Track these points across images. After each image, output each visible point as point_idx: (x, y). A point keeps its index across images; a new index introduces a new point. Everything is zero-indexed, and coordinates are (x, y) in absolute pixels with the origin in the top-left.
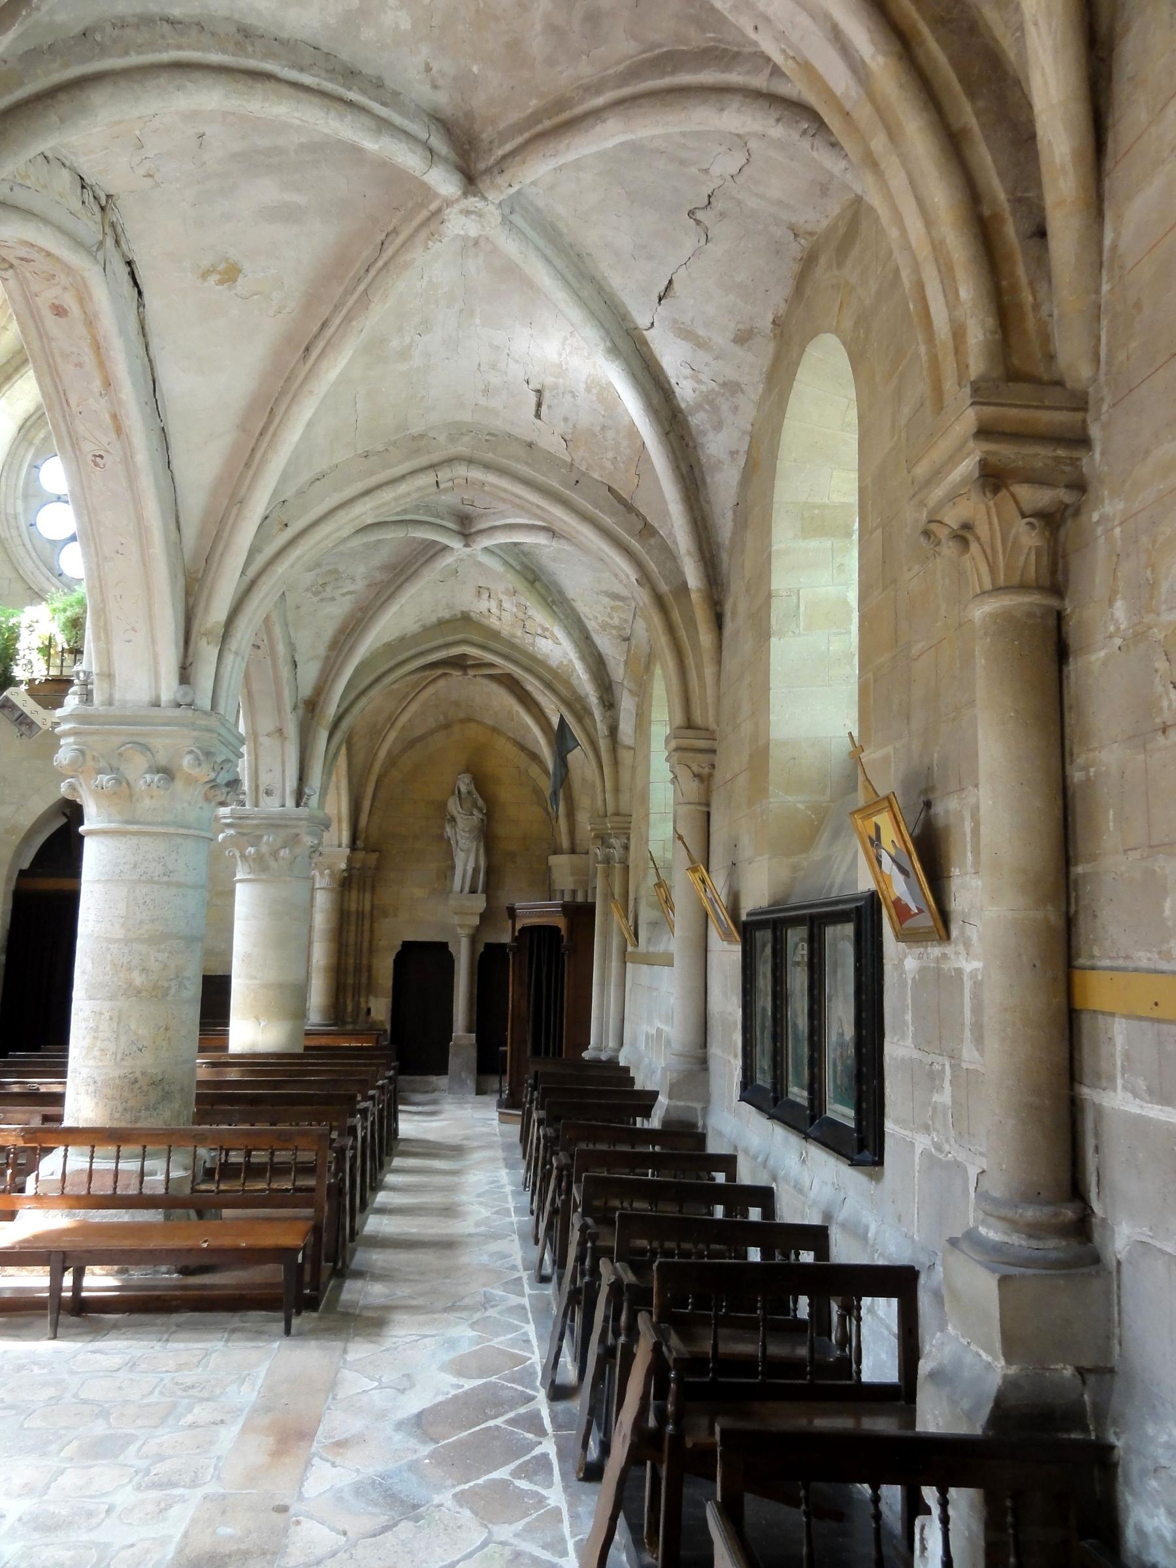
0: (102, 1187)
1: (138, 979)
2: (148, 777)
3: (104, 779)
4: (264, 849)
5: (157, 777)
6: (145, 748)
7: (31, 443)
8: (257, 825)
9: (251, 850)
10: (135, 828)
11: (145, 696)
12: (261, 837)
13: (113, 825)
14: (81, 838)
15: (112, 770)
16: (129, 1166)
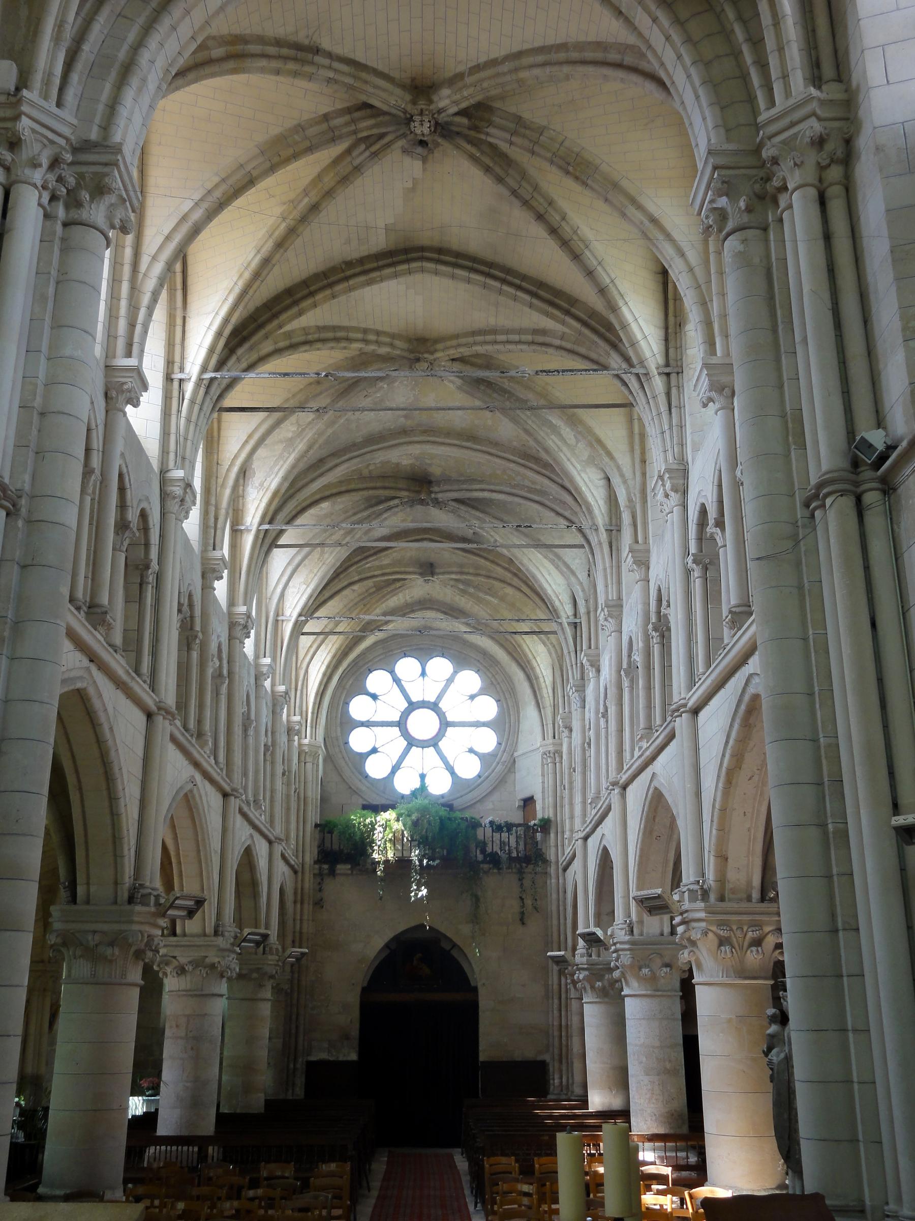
0: (682, 1162)
1: (668, 1066)
2: (664, 969)
3: (645, 971)
4: (606, 983)
5: (668, 969)
6: (661, 956)
7: (344, 688)
8: (601, 969)
9: (599, 984)
10: (660, 993)
11: (658, 931)
12: (603, 976)
13: (649, 992)
14: (622, 998)
15: (647, 966)
16: (683, 1154)
